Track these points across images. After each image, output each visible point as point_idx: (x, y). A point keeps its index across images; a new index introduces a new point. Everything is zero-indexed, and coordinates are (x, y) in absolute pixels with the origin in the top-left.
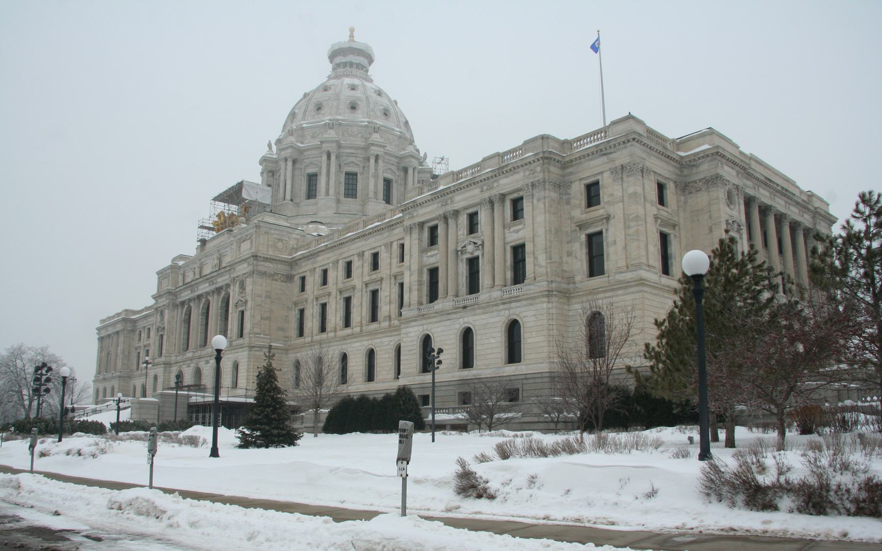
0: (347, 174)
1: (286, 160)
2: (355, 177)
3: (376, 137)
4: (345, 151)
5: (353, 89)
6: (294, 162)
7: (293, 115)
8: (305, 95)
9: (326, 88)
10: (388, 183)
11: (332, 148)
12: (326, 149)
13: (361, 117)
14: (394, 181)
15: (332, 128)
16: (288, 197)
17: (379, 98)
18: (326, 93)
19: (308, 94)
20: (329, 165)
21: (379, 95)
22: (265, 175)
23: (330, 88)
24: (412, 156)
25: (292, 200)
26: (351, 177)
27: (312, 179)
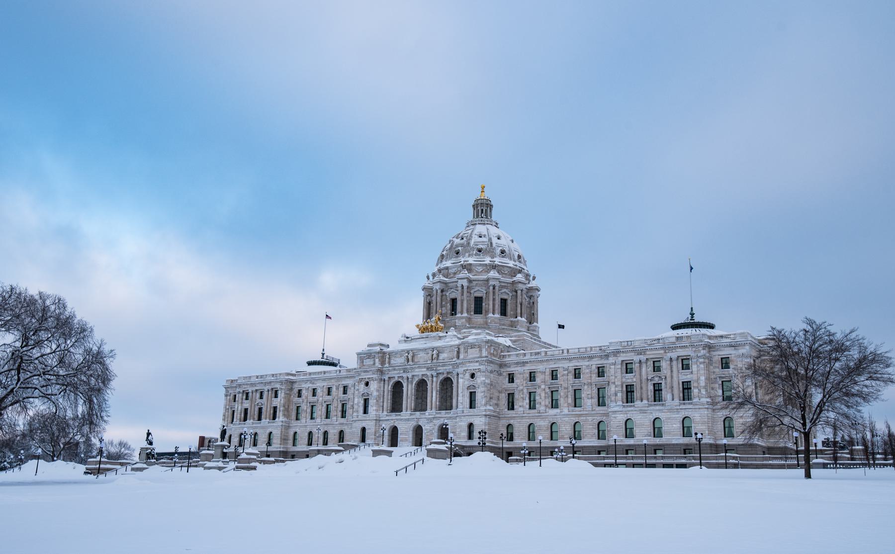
4: (450, 285)
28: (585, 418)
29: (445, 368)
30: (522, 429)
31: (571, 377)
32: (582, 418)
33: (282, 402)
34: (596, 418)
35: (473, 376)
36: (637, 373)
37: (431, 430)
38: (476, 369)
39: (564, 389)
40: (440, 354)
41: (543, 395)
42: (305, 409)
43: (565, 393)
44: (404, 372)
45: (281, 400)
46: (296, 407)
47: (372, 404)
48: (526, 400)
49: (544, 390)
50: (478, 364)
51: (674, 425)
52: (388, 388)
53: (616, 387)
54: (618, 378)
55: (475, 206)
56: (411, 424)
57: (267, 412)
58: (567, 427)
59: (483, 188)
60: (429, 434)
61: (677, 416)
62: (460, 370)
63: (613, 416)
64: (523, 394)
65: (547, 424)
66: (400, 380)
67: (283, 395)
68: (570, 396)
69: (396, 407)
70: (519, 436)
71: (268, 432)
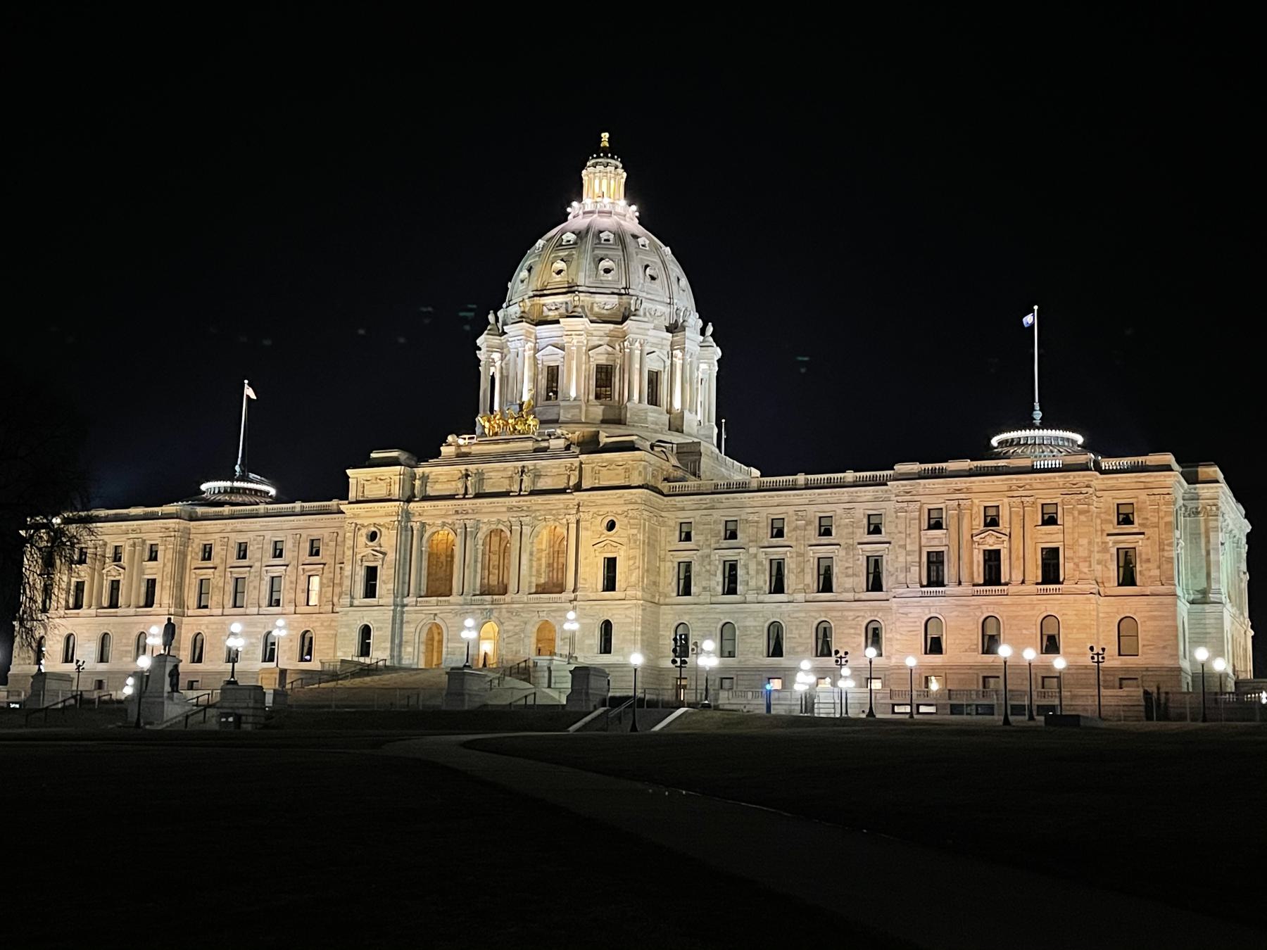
31: (812, 532)
33: (168, 569)
36: (953, 529)
37: (516, 634)
39: (797, 556)
41: (753, 567)
42: (221, 584)
43: (798, 565)
45: (165, 565)
46: (198, 582)
47: (384, 578)
48: (716, 575)
49: (755, 556)
51: (1024, 632)
53: (908, 554)
54: (912, 536)
57: (131, 592)
60: (511, 640)
64: (709, 564)
65: (760, 624)
67: (169, 555)
68: (808, 570)
71: (136, 633)
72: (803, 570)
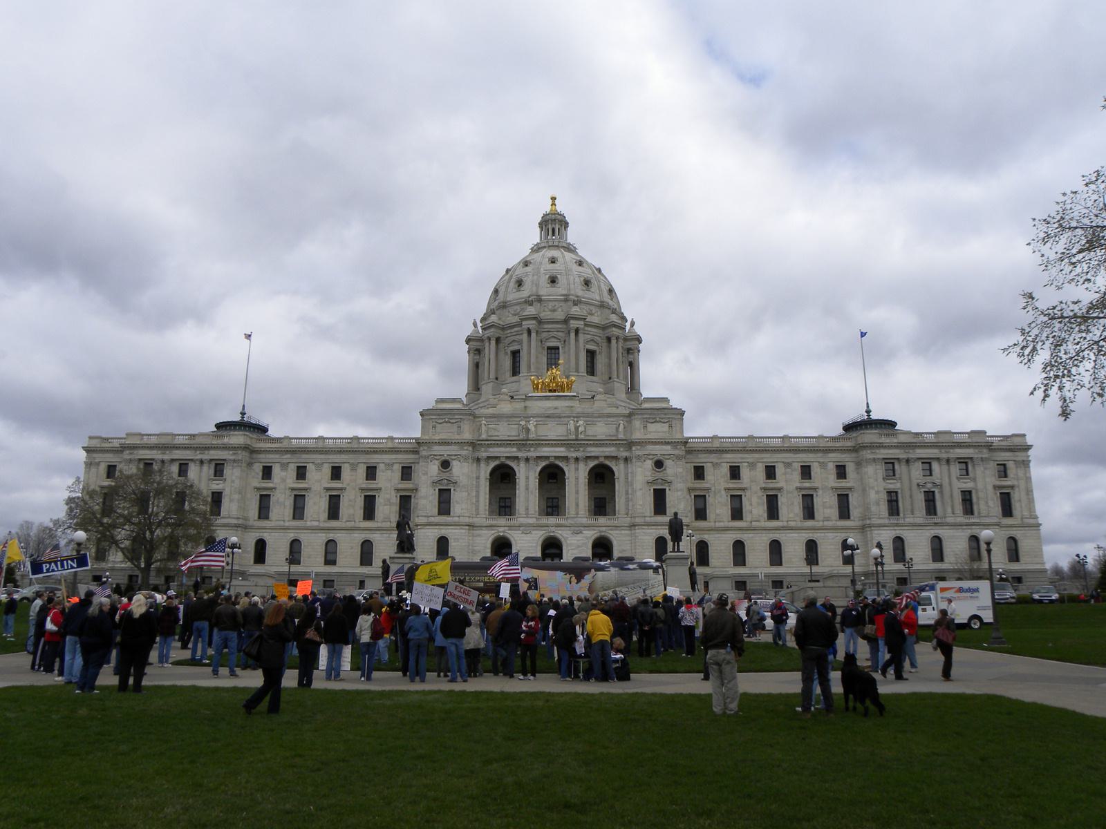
0: (549, 348)
1: (489, 339)
2: (557, 351)
3: (575, 310)
4: (546, 326)
5: (553, 262)
6: (498, 340)
7: (496, 291)
8: (508, 271)
9: (526, 263)
10: (591, 354)
11: (532, 324)
12: (526, 327)
13: (561, 289)
14: (598, 352)
15: (531, 305)
16: (492, 376)
17: (580, 269)
18: (527, 268)
19: (510, 270)
20: (530, 341)
21: (580, 265)
22: (472, 355)
23: (531, 263)
24: (615, 326)
25: (497, 379)
26: (553, 351)
27: (515, 354)
28: (823, 534)
29: (601, 449)
30: (722, 548)
32: (819, 534)
34: (839, 534)
35: (659, 464)
38: (664, 455)
40: (588, 427)
41: (755, 500)
44: (519, 450)
50: (669, 447)
52: (485, 470)
55: (541, 224)
56: (539, 535)
58: (796, 547)
59: (554, 199)
61: (963, 534)
62: (637, 451)
63: (876, 532)
64: (721, 497)
66: (509, 463)
69: (504, 505)
70: (719, 558)
72: (793, 504)
